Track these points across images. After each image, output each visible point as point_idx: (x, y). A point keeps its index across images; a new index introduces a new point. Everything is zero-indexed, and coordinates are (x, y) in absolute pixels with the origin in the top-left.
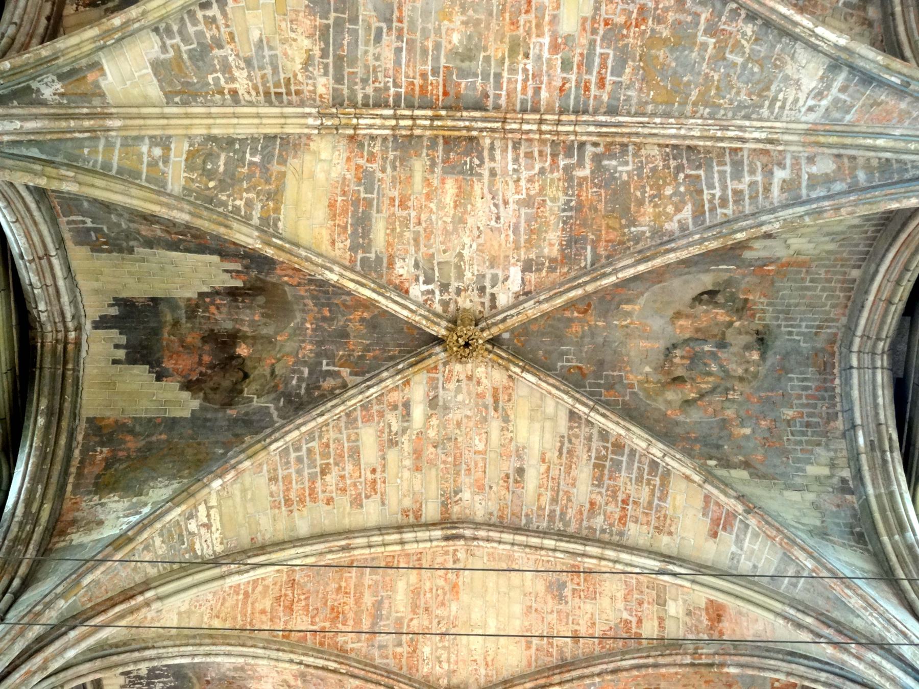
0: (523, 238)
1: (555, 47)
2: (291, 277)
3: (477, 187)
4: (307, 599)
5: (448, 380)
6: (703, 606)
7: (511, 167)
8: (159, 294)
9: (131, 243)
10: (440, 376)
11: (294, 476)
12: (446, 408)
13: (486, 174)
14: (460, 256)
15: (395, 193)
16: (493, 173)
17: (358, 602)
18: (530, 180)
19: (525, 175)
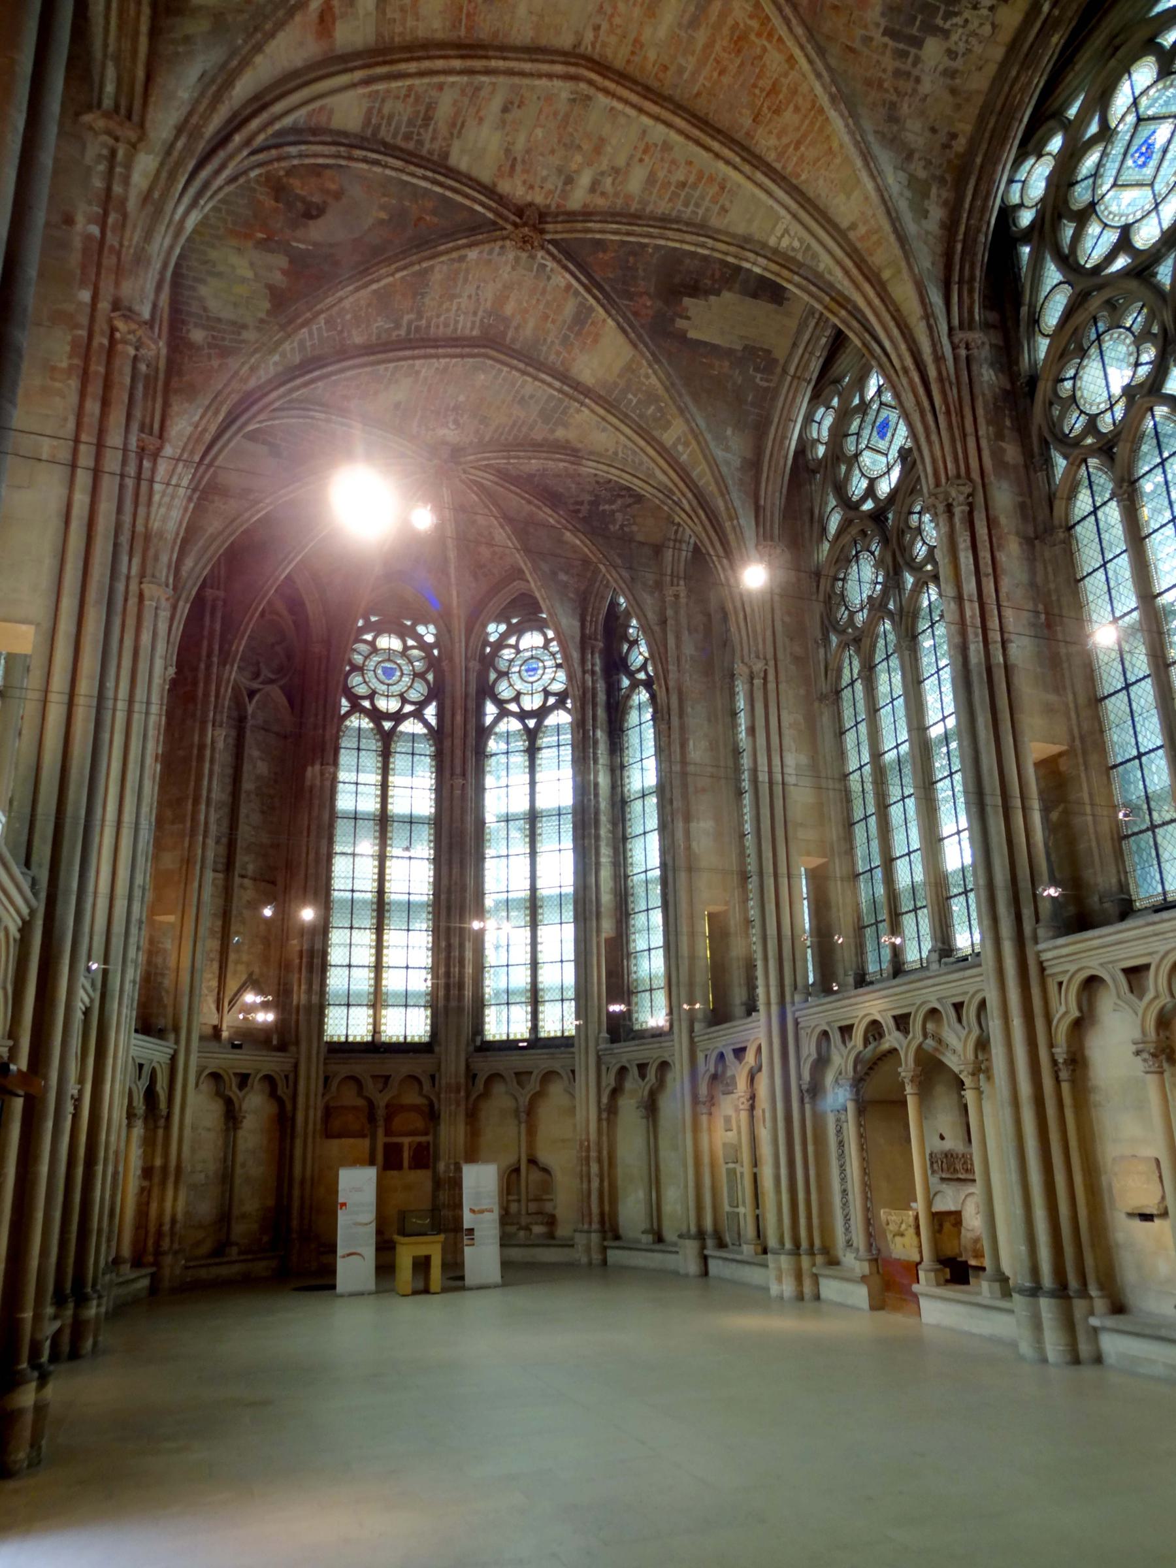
0: (462, 275)
1: (418, 373)
2: (646, 307)
3: (489, 304)
4: (755, 86)
5: (550, 192)
6: (338, 23)
7: (461, 318)
8: (748, 300)
9: (739, 354)
10: (556, 198)
11: (708, 199)
12: (560, 170)
13: (480, 313)
14: (513, 269)
15: (549, 325)
16: (475, 314)
17: (709, 45)
18: (448, 310)
19: (452, 314)
